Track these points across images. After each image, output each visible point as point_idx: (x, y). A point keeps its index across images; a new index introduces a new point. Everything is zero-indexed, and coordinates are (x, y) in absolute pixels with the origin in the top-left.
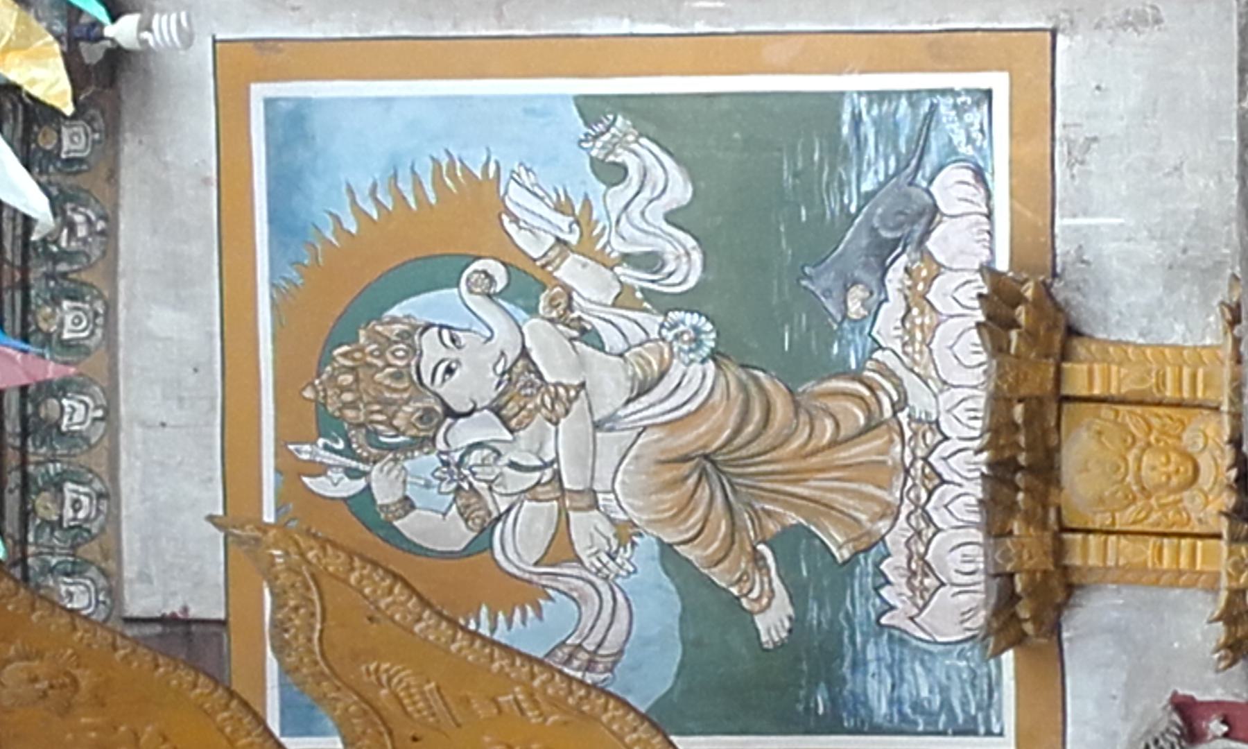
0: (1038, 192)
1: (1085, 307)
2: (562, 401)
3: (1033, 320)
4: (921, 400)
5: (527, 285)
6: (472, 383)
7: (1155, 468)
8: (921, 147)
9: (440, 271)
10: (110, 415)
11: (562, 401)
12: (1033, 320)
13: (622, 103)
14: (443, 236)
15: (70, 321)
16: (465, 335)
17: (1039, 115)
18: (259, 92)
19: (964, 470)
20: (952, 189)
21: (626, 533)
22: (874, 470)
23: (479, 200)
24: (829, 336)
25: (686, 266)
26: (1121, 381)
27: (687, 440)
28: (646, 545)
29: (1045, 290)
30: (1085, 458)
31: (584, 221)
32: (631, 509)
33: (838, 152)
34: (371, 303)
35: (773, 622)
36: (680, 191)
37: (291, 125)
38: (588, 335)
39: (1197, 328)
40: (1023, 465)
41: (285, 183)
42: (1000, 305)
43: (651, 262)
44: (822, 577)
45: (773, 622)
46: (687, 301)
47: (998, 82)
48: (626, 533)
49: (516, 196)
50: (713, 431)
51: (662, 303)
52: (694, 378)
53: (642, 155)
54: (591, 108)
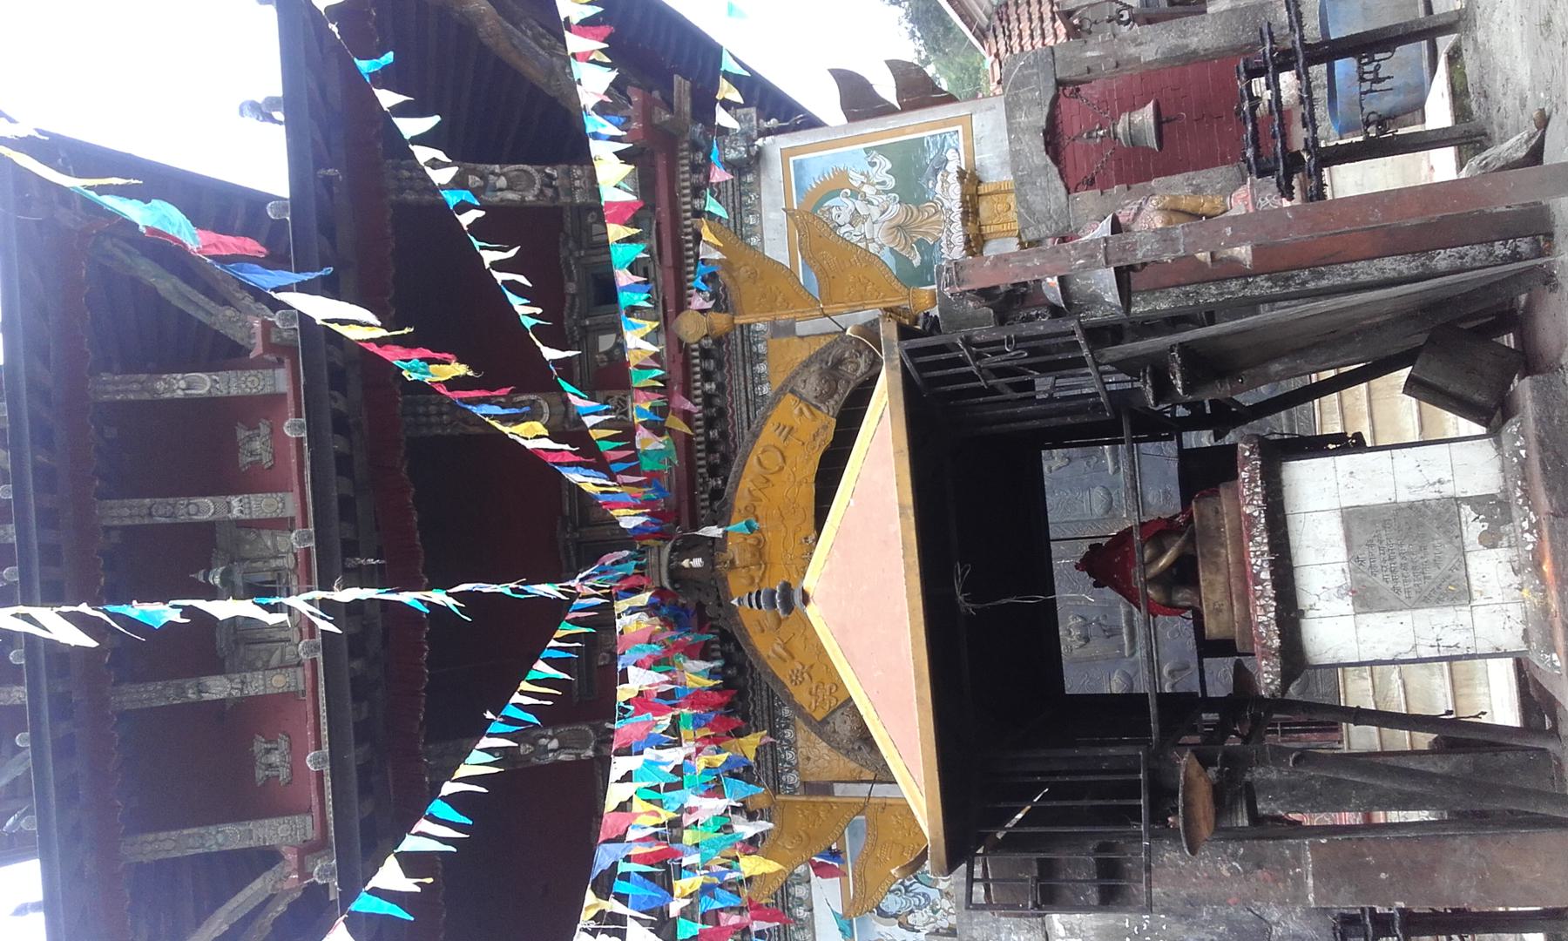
0: (970, 152)
1: (983, 176)
2: (865, 218)
3: (970, 179)
4: (947, 204)
5: (855, 193)
7: (1000, 207)
9: (835, 193)
10: (762, 240)
11: (865, 218)
12: (970, 179)
13: (874, 148)
14: (837, 185)
15: (751, 220)
16: (841, 208)
17: (969, 134)
19: (957, 216)
20: (950, 154)
21: (881, 247)
22: (938, 222)
23: (842, 176)
25: (891, 182)
26: (991, 189)
27: (894, 223)
28: (887, 248)
29: (973, 174)
30: (985, 208)
31: (867, 176)
32: (882, 241)
33: (924, 150)
34: (820, 204)
36: (889, 166)
37: (799, 166)
38: (870, 203)
39: (1007, 177)
40: (970, 210)
42: (962, 175)
43: (883, 183)
44: (927, 249)
45: (916, 262)
46: (891, 191)
47: (959, 128)
48: (881, 247)
49: (852, 174)
51: (886, 192)
52: (895, 208)
53: (880, 159)
54: (867, 150)
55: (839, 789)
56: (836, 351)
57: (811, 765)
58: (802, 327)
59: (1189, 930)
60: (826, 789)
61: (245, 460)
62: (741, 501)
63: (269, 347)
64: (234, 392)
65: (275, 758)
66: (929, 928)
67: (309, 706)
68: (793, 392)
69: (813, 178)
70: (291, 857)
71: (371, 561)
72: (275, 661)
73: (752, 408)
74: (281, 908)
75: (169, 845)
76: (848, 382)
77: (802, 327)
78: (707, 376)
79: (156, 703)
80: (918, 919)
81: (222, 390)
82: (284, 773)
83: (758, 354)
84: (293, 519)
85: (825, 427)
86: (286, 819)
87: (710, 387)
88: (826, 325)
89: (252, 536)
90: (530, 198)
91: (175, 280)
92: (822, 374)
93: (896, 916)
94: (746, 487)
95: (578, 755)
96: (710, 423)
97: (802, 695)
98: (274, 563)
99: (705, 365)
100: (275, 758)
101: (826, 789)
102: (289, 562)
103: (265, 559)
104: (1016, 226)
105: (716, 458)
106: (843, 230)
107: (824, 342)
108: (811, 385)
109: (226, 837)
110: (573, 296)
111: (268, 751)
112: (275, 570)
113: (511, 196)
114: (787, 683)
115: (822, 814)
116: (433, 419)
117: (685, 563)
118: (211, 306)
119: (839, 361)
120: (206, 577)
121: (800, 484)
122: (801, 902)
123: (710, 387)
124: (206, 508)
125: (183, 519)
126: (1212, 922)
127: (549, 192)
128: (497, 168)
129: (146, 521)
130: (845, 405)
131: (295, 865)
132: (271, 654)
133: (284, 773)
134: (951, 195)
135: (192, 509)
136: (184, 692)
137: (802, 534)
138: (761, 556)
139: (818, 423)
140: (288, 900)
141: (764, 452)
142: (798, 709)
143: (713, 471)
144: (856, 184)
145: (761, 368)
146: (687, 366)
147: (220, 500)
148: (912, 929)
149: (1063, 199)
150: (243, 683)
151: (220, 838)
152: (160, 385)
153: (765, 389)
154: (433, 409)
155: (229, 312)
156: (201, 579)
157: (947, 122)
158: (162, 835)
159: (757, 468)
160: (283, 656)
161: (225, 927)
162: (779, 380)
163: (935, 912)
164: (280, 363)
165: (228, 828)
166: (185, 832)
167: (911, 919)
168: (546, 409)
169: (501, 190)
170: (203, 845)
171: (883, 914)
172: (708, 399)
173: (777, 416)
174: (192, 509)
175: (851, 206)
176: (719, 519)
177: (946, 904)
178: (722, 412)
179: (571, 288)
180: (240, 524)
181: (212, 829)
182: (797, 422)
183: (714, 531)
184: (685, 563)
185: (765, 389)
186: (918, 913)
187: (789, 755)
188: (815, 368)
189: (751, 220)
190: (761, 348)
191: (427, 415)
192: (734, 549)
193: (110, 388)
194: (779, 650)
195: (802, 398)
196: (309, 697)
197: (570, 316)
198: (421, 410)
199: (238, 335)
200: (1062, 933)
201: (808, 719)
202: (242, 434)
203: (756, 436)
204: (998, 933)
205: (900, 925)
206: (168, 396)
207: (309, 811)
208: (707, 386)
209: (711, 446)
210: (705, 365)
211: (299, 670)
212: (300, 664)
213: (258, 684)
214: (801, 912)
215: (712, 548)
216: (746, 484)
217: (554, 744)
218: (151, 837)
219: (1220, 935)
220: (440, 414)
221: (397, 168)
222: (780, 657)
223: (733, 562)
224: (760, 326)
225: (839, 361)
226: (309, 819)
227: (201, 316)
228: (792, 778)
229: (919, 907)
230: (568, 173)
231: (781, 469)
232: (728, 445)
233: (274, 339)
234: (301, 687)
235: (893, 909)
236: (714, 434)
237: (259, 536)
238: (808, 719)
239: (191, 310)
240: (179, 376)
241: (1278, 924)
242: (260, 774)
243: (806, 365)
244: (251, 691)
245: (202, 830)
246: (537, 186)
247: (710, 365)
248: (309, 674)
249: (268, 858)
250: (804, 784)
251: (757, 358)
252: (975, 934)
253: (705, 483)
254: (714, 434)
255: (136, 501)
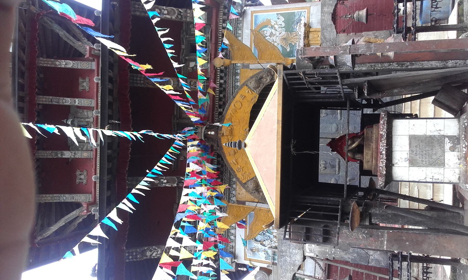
0: (309, 18)
1: (311, 26)
3: (308, 26)
4: (300, 33)
5: (272, 27)
6: (268, 34)
7: (316, 36)
8: (301, 15)
9: (266, 26)
10: (242, 38)
12: (308, 26)
14: (267, 24)
15: (240, 32)
16: (267, 31)
17: (309, 12)
18: (254, 14)
20: (303, 18)
21: (278, 44)
22: (296, 39)
23: (269, 21)
24: (293, 29)
25: (283, 25)
29: (308, 25)
30: (311, 36)
31: (276, 22)
33: (295, 16)
34: (261, 29)
35: (288, 50)
37: (256, 17)
38: (276, 30)
40: (306, 36)
41: (255, 21)
42: (305, 25)
43: (281, 25)
44: (292, 46)
45: (288, 50)
46: (283, 27)
47: (306, 10)
48: (278, 44)
49: (272, 21)
50: (285, 37)
51: (282, 28)
52: (284, 33)
54: (277, 14)
55: (247, 203)
56: (261, 75)
57: (239, 196)
58: (251, 66)
59: (346, 254)
60: (244, 203)
61: (81, 88)
62: (228, 116)
63: (91, 55)
64: (79, 67)
65: (82, 177)
66: (269, 246)
67: (94, 163)
68: (247, 85)
69: (260, 21)
70: (85, 206)
71: (116, 122)
72: (85, 149)
73: (234, 89)
74: (81, 220)
75: (49, 198)
76: (264, 84)
77: (251, 66)
78: (221, 78)
79: (49, 157)
80: (266, 243)
81: (76, 67)
82: (85, 181)
83: (237, 73)
84: (93, 107)
85: (255, 97)
86: (84, 195)
87: (222, 81)
88: (259, 66)
89: (81, 111)
90: (174, 18)
91: (64, 32)
92: (256, 81)
93: (260, 241)
94: (229, 112)
95: (172, 185)
96: (221, 92)
97: (239, 175)
98: (87, 120)
99: (221, 74)
100: (82, 177)
101: (244, 203)
102: (91, 120)
103: (85, 118)
104: (320, 42)
105: (221, 103)
106: (267, 38)
107: (258, 71)
108: (252, 84)
109: (66, 198)
110: (184, 49)
111: (81, 174)
112: (87, 122)
113: (168, 16)
114: (236, 171)
115: (242, 210)
116: (138, 82)
117: (209, 133)
118: (74, 40)
119: (262, 78)
120: (66, 122)
121: (246, 113)
122: (233, 234)
123: (222, 81)
124: (68, 101)
125: (61, 103)
126: (352, 253)
127: (180, 17)
128: (165, 8)
129: (50, 103)
130: (262, 91)
131: (86, 208)
132: (84, 146)
133: (85, 181)
134: (301, 30)
135: (64, 101)
136: (57, 155)
137: (245, 128)
138: (232, 133)
139: (253, 96)
140: (83, 218)
141: (236, 102)
142: (238, 179)
143: (220, 106)
144: (273, 24)
145: (238, 77)
146: (216, 74)
147: (73, 99)
148: (264, 246)
149: (335, 35)
150: (75, 154)
151: (65, 198)
152: (57, 63)
153: (238, 84)
154: (138, 78)
155: (80, 43)
156: (65, 122)
157: (302, 8)
158: (48, 195)
159: (233, 107)
160: (87, 147)
161: (64, 224)
162: (243, 81)
163: (271, 241)
164: (94, 60)
165: (67, 195)
166: (54, 195)
167: (264, 243)
168: (172, 83)
169: (165, 14)
170: (59, 200)
171: (256, 240)
172: (221, 85)
173: (241, 92)
174: (64, 101)
175: (271, 31)
176: (221, 121)
177: (275, 239)
178: (225, 89)
179: (183, 47)
180: (78, 107)
181: (62, 195)
182: (247, 95)
183: (218, 124)
184: (209, 133)
185: (238, 84)
186: (266, 241)
187: (234, 192)
188: (254, 79)
189: (240, 32)
190: (239, 71)
191: (137, 80)
192: (224, 130)
193: (43, 62)
194: (234, 161)
195: (249, 88)
196: (94, 160)
197: (182, 55)
198: (135, 78)
199: (82, 50)
200: (308, 251)
201: (241, 182)
202: (81, 80)
203: (234, 97)
204: (290, 249)
205: (261, 244)
206: (60, 66)
207: (91, 193)
208: (221, 81)
209: (220, 99)
210: (221, 74)
211: (92, 152)
212: (92, 150)
213: (79, 155)
214: (232, 237)
215: (217, 129)
216: (229, 111)
217: (165, 181)
218: (44, 196)
219: (354, 257)
220: (140, 80)
221: (135, 4)
222: (234, 163)
223: (223, 134)
224: (239, 65)
225: (262, 78)
226: (91, 195)
227: (71, 43)
228: (234, 199)
229: (267, 240)
230: (186, 11)
231: (241, 108)
232: (225, 99)
233: (92, 53)
234: (92, 157)
235: (259, 239)
236: (222, 95)
237: (83, 111)
238: (241, 182)
239: (68, 41)
240: (63, 61)
241: (372, 255)
242: (78, 181)
243: (252, 78)
244: (77, 156)
245: (59, 195)
246: (176, 14)
247: (223, 75)
248: (94, 154)
249: (78, 205)
250: (237, 201)
251: (237, 74)
252: (283, 249)
253: (217, 110)
254: (222, 95)
255: (48, 97)
